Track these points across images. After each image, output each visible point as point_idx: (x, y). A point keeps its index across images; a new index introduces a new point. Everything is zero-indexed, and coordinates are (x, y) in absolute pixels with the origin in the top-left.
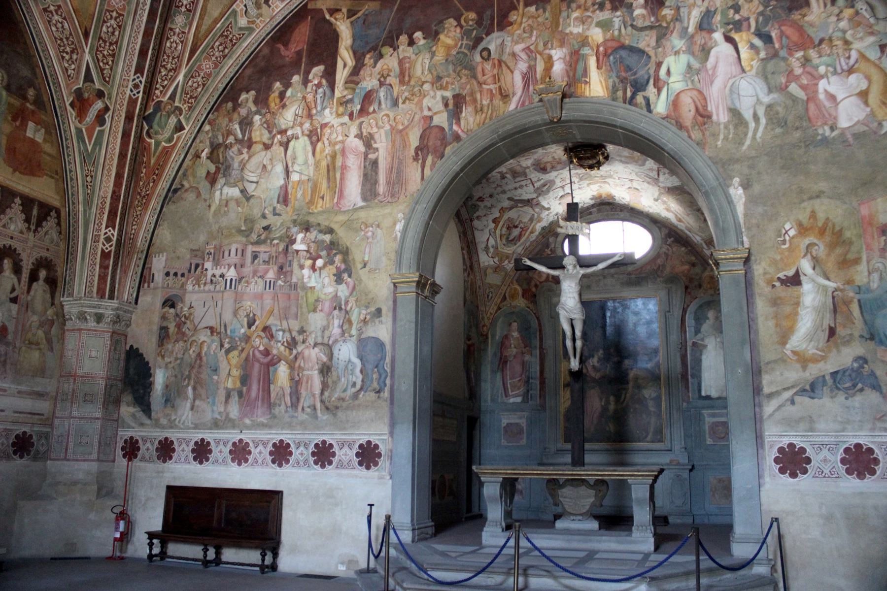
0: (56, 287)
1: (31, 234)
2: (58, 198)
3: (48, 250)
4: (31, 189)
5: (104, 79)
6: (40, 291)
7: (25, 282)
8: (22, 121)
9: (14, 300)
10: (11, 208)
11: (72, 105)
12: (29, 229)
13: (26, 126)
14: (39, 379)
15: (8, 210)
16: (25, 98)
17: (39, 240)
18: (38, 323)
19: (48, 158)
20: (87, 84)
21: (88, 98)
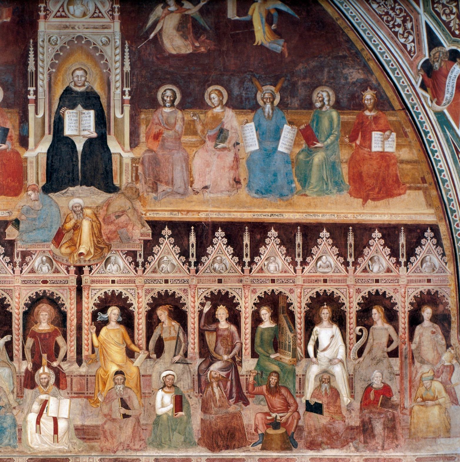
0: (449, 323)
1: (403, 268)
2: (432, 211)
3: (429, 281)
4: (392, 214)
5: (453, 34)
6: (427, 334)
7: (404, 329)
8: (363, 137)
9: (394, 354)
10: (369, 246)
11: (423, 86)
12: (398, 263)
13: (370, 139)
14: (442, 441)
15: (366, 250)
16: (361, 106)
17: (415, 272)
18: (431, 374)
19: (409, 166)
20: (434, 51)
21: (441, 67)
